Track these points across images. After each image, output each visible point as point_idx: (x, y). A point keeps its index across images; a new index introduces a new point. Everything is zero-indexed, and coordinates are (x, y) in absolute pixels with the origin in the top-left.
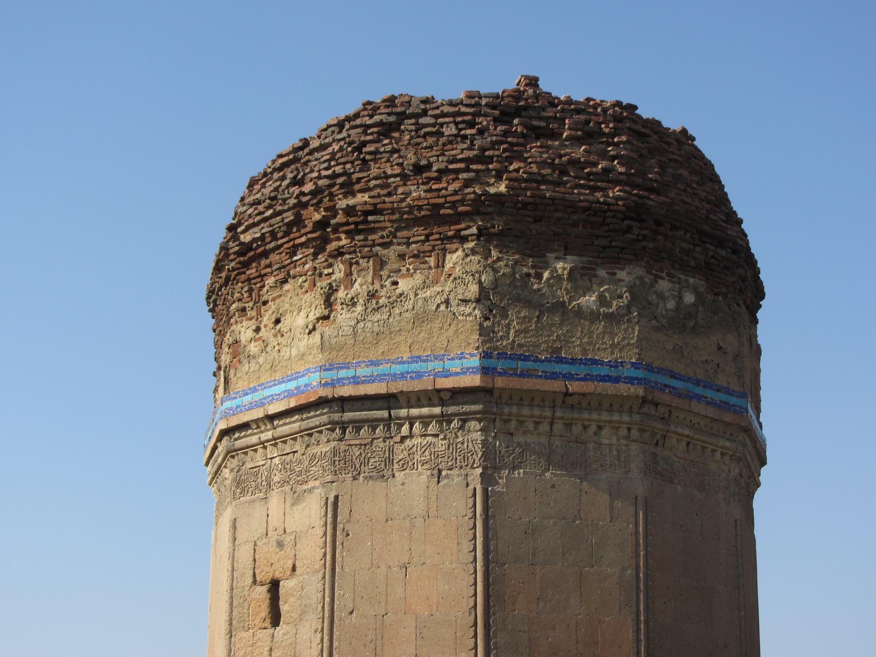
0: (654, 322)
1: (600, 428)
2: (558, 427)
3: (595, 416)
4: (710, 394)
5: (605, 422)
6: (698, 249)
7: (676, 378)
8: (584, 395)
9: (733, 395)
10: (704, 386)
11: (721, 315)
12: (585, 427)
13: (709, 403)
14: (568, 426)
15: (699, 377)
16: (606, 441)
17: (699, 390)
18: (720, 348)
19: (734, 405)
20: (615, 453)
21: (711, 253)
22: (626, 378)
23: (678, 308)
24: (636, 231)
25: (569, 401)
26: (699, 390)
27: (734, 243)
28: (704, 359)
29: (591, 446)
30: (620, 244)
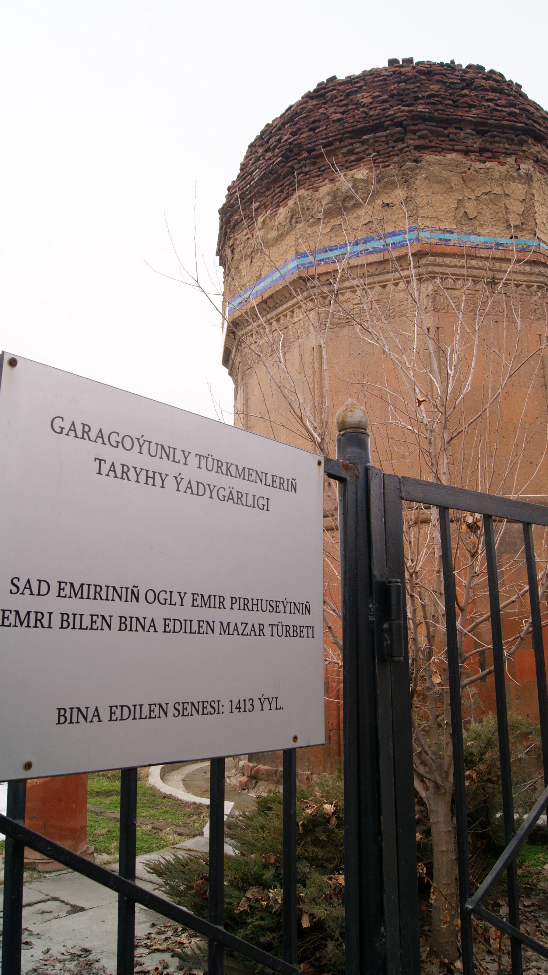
0: (312, 221)
1: (292, 312)
2: (274, 323)
3: (285, 306)
4: (370, 246)
5: (292, 307)
6: (355, 146)
7: (331, 250)
8: (271, 297)
9: (400, 235)
10: (365, 243)
11: (385, 180)
12: (286, 316)
13: (370, 253)
14: (278, 320)
15: (359, 238)
16: (296, 320)
17: (361, 247)
18: (388, 205)
19: (400, 242)
20: (302, 324)
21: (371, 141)
22: (289, 271)
23: (335, 197)
24: (296, 166)
25: (270, 303)
26: (361, 247)
27: (392, 120)
28: (367, 221)
29: (290, 327)
30: (287, 183)
